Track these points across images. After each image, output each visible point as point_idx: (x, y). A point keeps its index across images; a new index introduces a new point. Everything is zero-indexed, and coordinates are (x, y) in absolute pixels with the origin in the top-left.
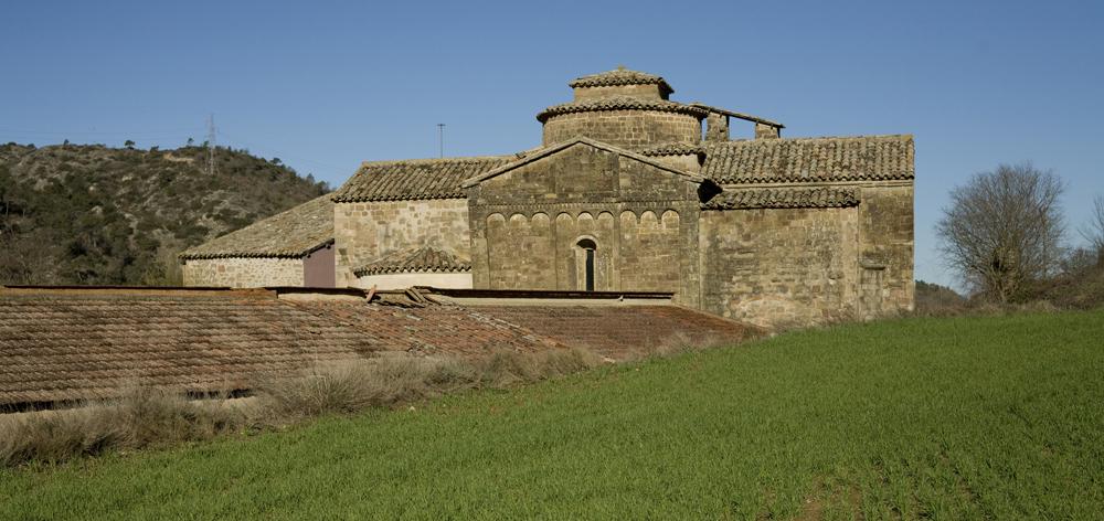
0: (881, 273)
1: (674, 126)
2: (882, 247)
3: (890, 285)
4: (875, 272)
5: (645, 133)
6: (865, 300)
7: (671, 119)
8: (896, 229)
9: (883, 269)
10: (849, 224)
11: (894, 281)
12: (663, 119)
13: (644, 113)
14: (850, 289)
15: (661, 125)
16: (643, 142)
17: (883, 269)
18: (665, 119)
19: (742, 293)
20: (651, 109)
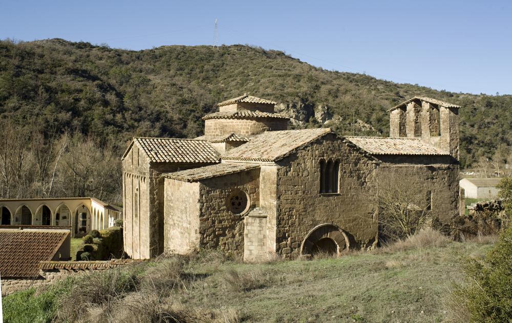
0: (264, 219)
1: (233, 126)
2: (266, 203)
3: (269, 228)
4: (258, 220)
5: (218, 130)
6: (249, 236)
7: (232, 122)
8: (271, 193)
9: (266, 217)
10: (194, 192)
11: (269, 225)
12: (227, 122)
13: (218, 120)
14: (194, 232)
15: (227, 126)
16: (217, 135)
17: (266, 217)
18: (229, 123)
19: (171, 225)
20: (221, 118)
